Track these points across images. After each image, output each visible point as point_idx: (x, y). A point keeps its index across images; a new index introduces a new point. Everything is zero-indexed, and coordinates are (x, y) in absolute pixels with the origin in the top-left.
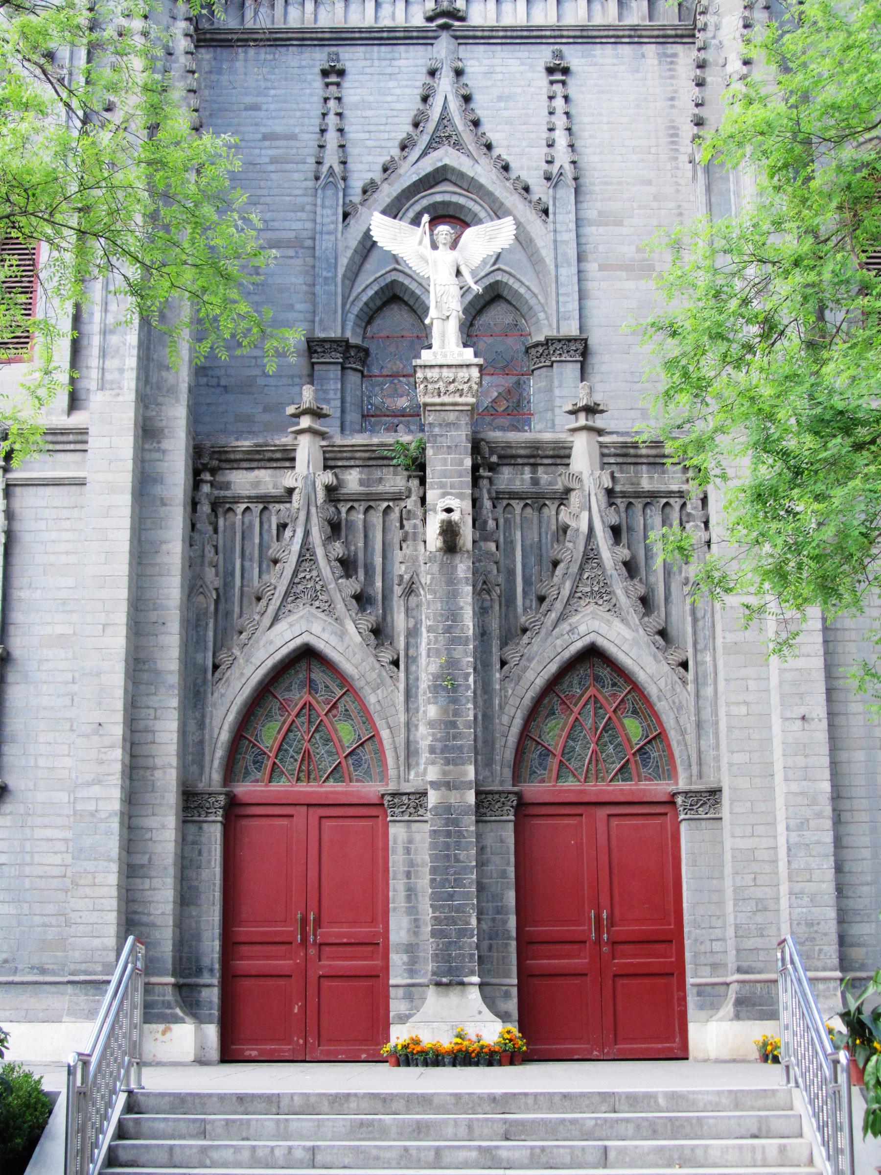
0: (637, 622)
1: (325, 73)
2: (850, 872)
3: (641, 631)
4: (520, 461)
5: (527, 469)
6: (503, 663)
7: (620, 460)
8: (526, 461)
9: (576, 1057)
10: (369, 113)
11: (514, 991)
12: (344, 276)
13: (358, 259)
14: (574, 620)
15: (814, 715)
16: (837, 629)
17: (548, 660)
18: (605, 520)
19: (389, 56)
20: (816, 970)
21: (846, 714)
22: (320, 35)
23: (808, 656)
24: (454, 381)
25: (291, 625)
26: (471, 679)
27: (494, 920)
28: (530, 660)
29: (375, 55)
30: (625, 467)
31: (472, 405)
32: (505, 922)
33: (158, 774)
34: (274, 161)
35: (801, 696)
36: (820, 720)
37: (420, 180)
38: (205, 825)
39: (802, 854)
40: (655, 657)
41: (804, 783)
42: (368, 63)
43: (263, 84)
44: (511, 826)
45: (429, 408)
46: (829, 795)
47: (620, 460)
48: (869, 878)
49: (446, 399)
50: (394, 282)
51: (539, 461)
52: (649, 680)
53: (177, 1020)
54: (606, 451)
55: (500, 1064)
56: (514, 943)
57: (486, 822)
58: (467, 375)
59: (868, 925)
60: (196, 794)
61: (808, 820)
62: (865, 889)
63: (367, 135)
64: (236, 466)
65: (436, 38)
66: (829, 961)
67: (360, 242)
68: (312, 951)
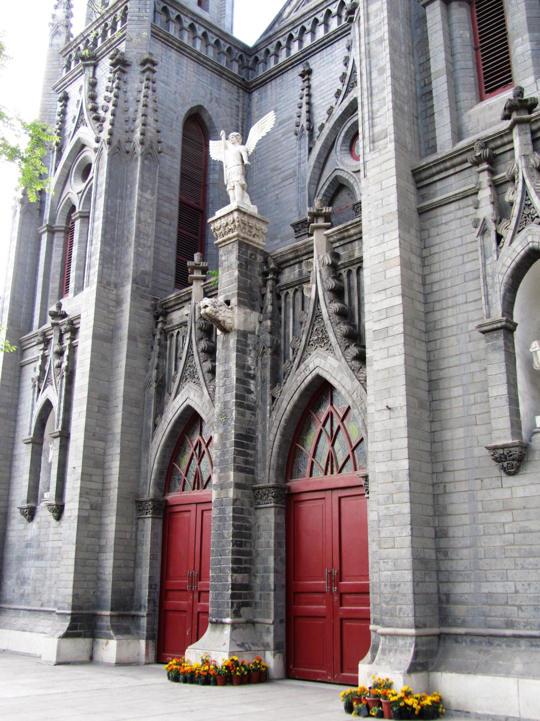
0: (341, 354)
1: (302, 75)
2: (453, 537)
3: (343, 360)
4: (292, 262)
5: (297, 266)
6: (273, 399)
7: (342, 242)
8: (294, 261)
9: (319, 679)
10: (323, 88)
11: (272, 628)
12: (310, 183)
13: (318, 171)
14: (306, 361)
15: (397, 404)
16: (443, 328)
17: (293, 392)
18: (325, 286)
19: (331, 51)
20: (398, 627)
21: (450, 398)
22: (298, 58)
23: (394, 356)
24: (227, 224)
25: (182, 396)
26: (234, 414)
27: (263, 576)
28: (284, 395)
29: (325, 54)
30: (346, 246)
31: (238, 236)
32: (268, 578)
33: (111, 492)
34: (284, 134)
35: (388, 390)
36: (401, 408)
37: (343, 113)
38: (146, 520)
39: (388, 525)
40: (351, 377)
41: (390, 463)
42: (322, 60)
43: (278, 97)
44: (273, 510)
45: (219, 246)
46: (407, 472)
47: (342, 242)
48: (468, 542)
49: (226, 237)
50: (336, 177)
51: (301, 259)
52: (347, 395)
53: (111, 638)
54: (332, 239)
55: (216, 684)
56: (272, 593)
57: (260, 508)
58: (231, 219)
59: (468, 584)
60: (141, 502)
61: (392, 494)
62: (465, 552)
63: (322, 100)
64: (173, 309)
65: (350, 29)
66: (407, 619)
67: (316, 161)
68: (196, 596)
